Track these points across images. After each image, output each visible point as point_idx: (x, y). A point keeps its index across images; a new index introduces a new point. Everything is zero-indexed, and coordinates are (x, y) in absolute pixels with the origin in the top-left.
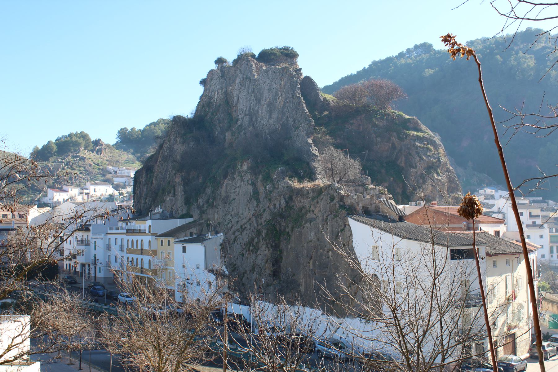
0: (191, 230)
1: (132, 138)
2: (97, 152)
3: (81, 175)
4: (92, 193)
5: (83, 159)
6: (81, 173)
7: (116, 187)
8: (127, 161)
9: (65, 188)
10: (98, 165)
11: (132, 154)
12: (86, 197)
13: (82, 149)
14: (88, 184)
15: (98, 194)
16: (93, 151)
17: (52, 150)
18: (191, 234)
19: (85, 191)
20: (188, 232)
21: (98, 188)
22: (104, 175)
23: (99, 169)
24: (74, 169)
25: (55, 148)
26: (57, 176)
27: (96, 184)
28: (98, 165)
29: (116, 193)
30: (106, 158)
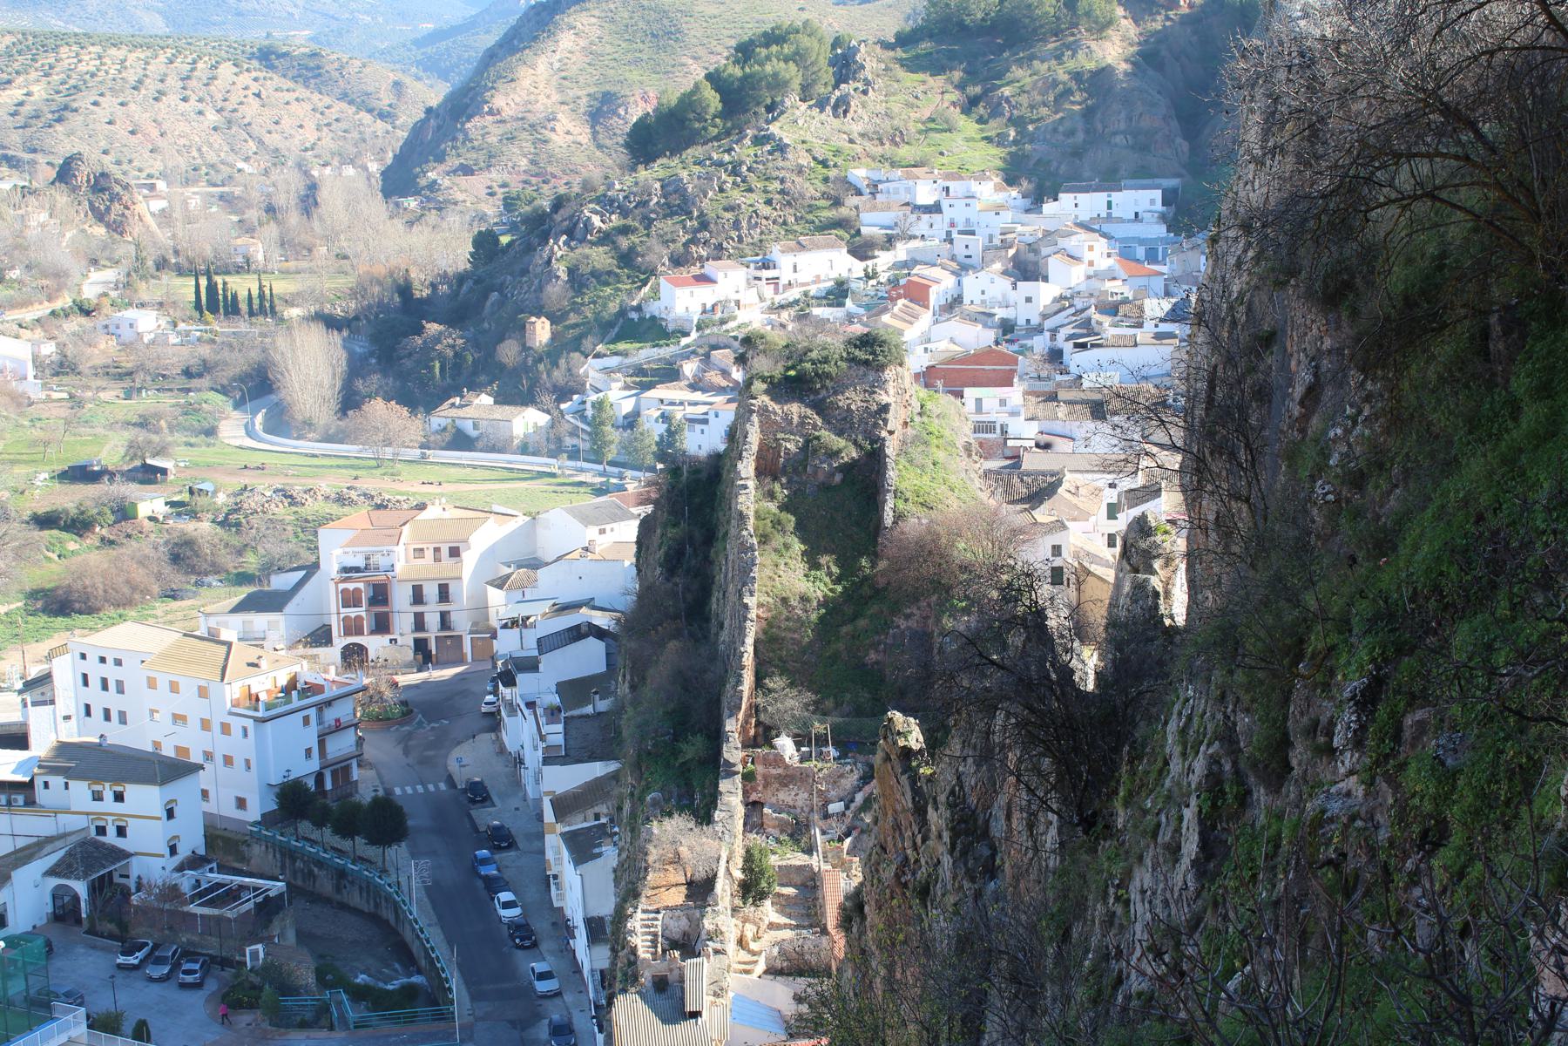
0: (596, 809)
1: (968, 20)
2: (835, 108)
3: (766, 211)
4: (785, 275)
5: (781, 148)
6: (769, 202)
7: (861, 250)
8: (935, 125)
9: (710, 268)
10: (824, 164)
11: (961, 87)
12: (768, 291)
13: (792, 99)
14: (775, 252)
15: (804, 276)
16: (821, 105)
17: (705, 109)
18: (597, 817)
19: (766, 274)
20: (590, 813)
21: (803, 259)
22: (837, 202)
23: (826, 180)
24: (750, 190)
25: (713, 100)
26: (702, 215)
27: (802, 247)
28: (824, 164)
29: (858, 267)
30: (857, 128)
